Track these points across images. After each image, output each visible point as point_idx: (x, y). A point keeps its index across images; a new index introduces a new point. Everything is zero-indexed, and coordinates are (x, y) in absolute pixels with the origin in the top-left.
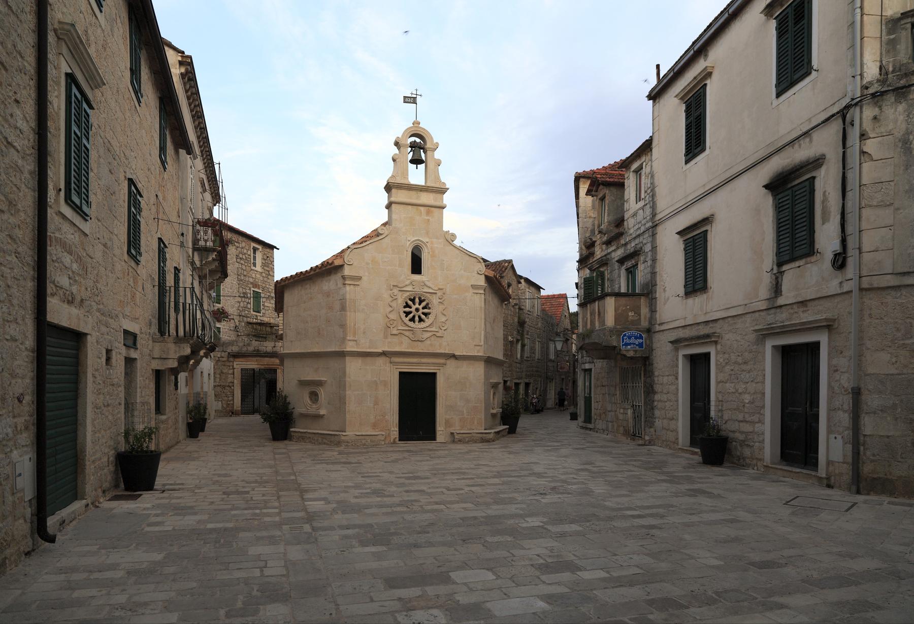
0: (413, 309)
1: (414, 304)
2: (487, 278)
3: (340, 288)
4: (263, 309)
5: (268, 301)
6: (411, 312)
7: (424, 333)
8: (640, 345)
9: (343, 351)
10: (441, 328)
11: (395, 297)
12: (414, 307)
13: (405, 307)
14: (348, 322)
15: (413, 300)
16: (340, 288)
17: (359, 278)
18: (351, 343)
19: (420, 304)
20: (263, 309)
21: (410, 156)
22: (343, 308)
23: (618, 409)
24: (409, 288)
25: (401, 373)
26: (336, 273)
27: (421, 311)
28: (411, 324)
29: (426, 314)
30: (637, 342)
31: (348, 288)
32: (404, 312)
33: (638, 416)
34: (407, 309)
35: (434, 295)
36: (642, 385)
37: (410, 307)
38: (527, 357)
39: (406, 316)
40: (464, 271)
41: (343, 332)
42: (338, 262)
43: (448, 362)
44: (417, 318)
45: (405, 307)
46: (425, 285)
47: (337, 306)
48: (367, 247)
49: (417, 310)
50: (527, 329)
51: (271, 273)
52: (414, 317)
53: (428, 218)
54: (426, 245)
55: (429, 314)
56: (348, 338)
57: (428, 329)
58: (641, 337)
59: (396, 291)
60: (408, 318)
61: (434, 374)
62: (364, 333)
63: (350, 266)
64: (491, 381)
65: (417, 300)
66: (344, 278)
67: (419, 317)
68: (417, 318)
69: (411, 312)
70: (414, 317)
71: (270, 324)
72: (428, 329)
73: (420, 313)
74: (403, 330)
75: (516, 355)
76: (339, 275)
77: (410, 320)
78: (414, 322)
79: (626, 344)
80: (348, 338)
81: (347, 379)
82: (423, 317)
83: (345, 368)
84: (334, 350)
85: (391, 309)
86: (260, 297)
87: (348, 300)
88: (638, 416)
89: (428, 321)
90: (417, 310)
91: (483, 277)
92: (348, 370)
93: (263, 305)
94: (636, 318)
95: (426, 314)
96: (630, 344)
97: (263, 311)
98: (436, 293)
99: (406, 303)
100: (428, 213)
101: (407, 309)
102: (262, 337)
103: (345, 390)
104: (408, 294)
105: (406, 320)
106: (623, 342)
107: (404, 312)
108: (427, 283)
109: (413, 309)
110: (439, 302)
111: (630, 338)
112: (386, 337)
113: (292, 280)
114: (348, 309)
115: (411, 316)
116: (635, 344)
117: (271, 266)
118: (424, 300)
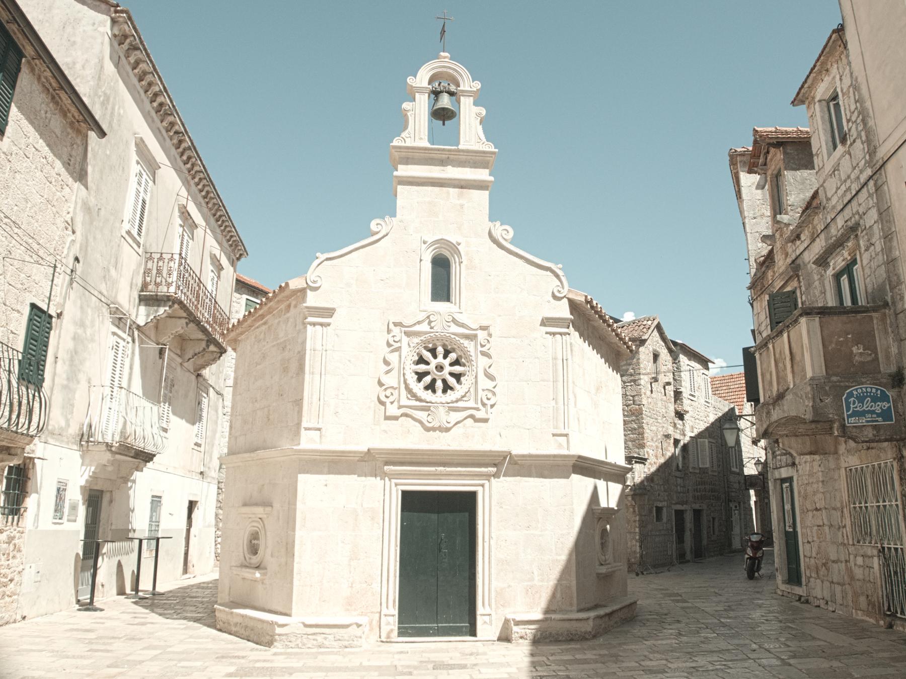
0: (432, 367)
6: (427, 373)
8: (886, 415)
10: (485, 401)
12: (434, 363)
23: (852, 557)
24: (424, 327)
27: (448, 369)
28: (428, 395)
30: (878, 407)
33: (896, 573)
34: (422, 368)
36: (899, 503)
37: (427, 363)
44: (439, 385)
49: (440, 368)
57: (461, 404)
58: (884, 398)
65: (440, 350)
67: (444, 381)
68: (439, 385)
70: (434, 381)
72: (461, 404)
73: (445, 373)
77: (427, 388)
78: (434, 391)
79: (856, 414)
88: (896, 573)
89: (460, 390)
90: (440, 368)
94: (869, 359)
96: (862, 414)
101: (422, 368)
105: (418, 388)
106: (848, 409)
107: (417, 373)
108: (458, 317)
109: (432, 367)
111: (861, 399)
116: (873, 412)
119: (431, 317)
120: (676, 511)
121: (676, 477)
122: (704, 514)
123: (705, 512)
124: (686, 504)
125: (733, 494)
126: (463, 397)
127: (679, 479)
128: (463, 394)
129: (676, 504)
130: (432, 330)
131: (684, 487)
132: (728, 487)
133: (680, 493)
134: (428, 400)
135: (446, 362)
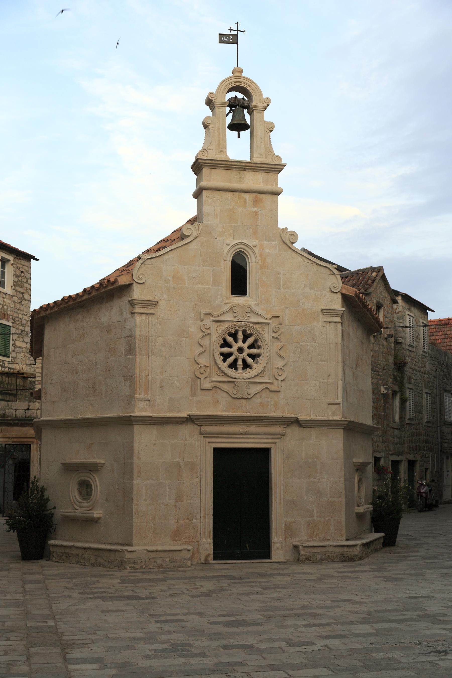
0: (234, 349)
1: (236, 341)
2: (345, 298)
3: (126, 319)
4: (14, 351)
5: (21, 339)
6: (230, 354)
7: (250, 385)
9: (130, 417)
11: (208, 331)
13: (222, 346)
14: (137, 371)
15: (234, 336)
16: (126, 319)
17: (154, 304)
18: (141, 404)
19: (244, 342)
20: (14, 351)
21: (229, 120)
22: (131, 350)
25: (215, 449)
26: (120, 297)
27: (247, 351)
28: (231, 372)
29: (253, 357)
31: (138, 319)
32: (222, 354)
34: (226, 350)
35: (266, 327)
38: (410, 419)
39: (224, 361)
40: (311, 289)
41: (130, 386)
42: (123, 281)
43: (289, 431)
44: (240, 363)
45: (222, 346)
46: (252, 311)
47: (122, 347)
48: (166, 257)
49: (241, 350)
50: (409, 374)
51: (26, 296)
52: (236, 361)
53: (256, 209)
54: (253, 251)
55: (259, 355)
56: (137, 396)
57: (258, 380)
59: (208, 321)
60: (226, 364)
61: (267, 451)
62: (161, 387)
63: (141, 285)
64: (354, 460)
65: (240, 335)
66: (132, 303)
68: (240, 363)
69: (230, 354)
70: (236, 361)
71: (22, 374)
72: (258, 380)
73: (245, 354)
74: (220, 382)
75: (393, 417)
76: (125, 299)
77: (230, 366)
78: (236, 369)
80: (137, 396)
81: (136, 461)
82: (249, 360)
83: (132, 443)
84: (115, 415)
85: (201, 350)
86: (10, 333)
87: (137, 337)
89: (257, 367)
91: (339, 296)
92: (136, 445)
93: (14, 345)
95: (253, 357)
97: (12, 354)
98: (268, 324)
99: (224, 340)
100: (256, 202)
101: (226, 350)
102: (11, 394)
103: (131, 478)
104: (227, 325)
105: (224, 366)
107: (222, 354)
109: (234, 349)
110: (274, 338)
112: (193, 394)
113: (56, 309)
114: (137, 350)
115: (231, 359)
117: (26, 285)
118: (250, 335)
119: (234, 308)
120: (392, 461)
121: (394, 428)
122: (418, 465)
123: (418, 462)
124: (402, 455)
125: (446, 445)
126: (259, 373)
127: (396, 431)
128: (260, 372)
129: (392, 454)
130: (235, 320)
131: (400, 438)
132: (441, 438)
133: (396, 444)
134: (233, 376)
135: (240, 344)
